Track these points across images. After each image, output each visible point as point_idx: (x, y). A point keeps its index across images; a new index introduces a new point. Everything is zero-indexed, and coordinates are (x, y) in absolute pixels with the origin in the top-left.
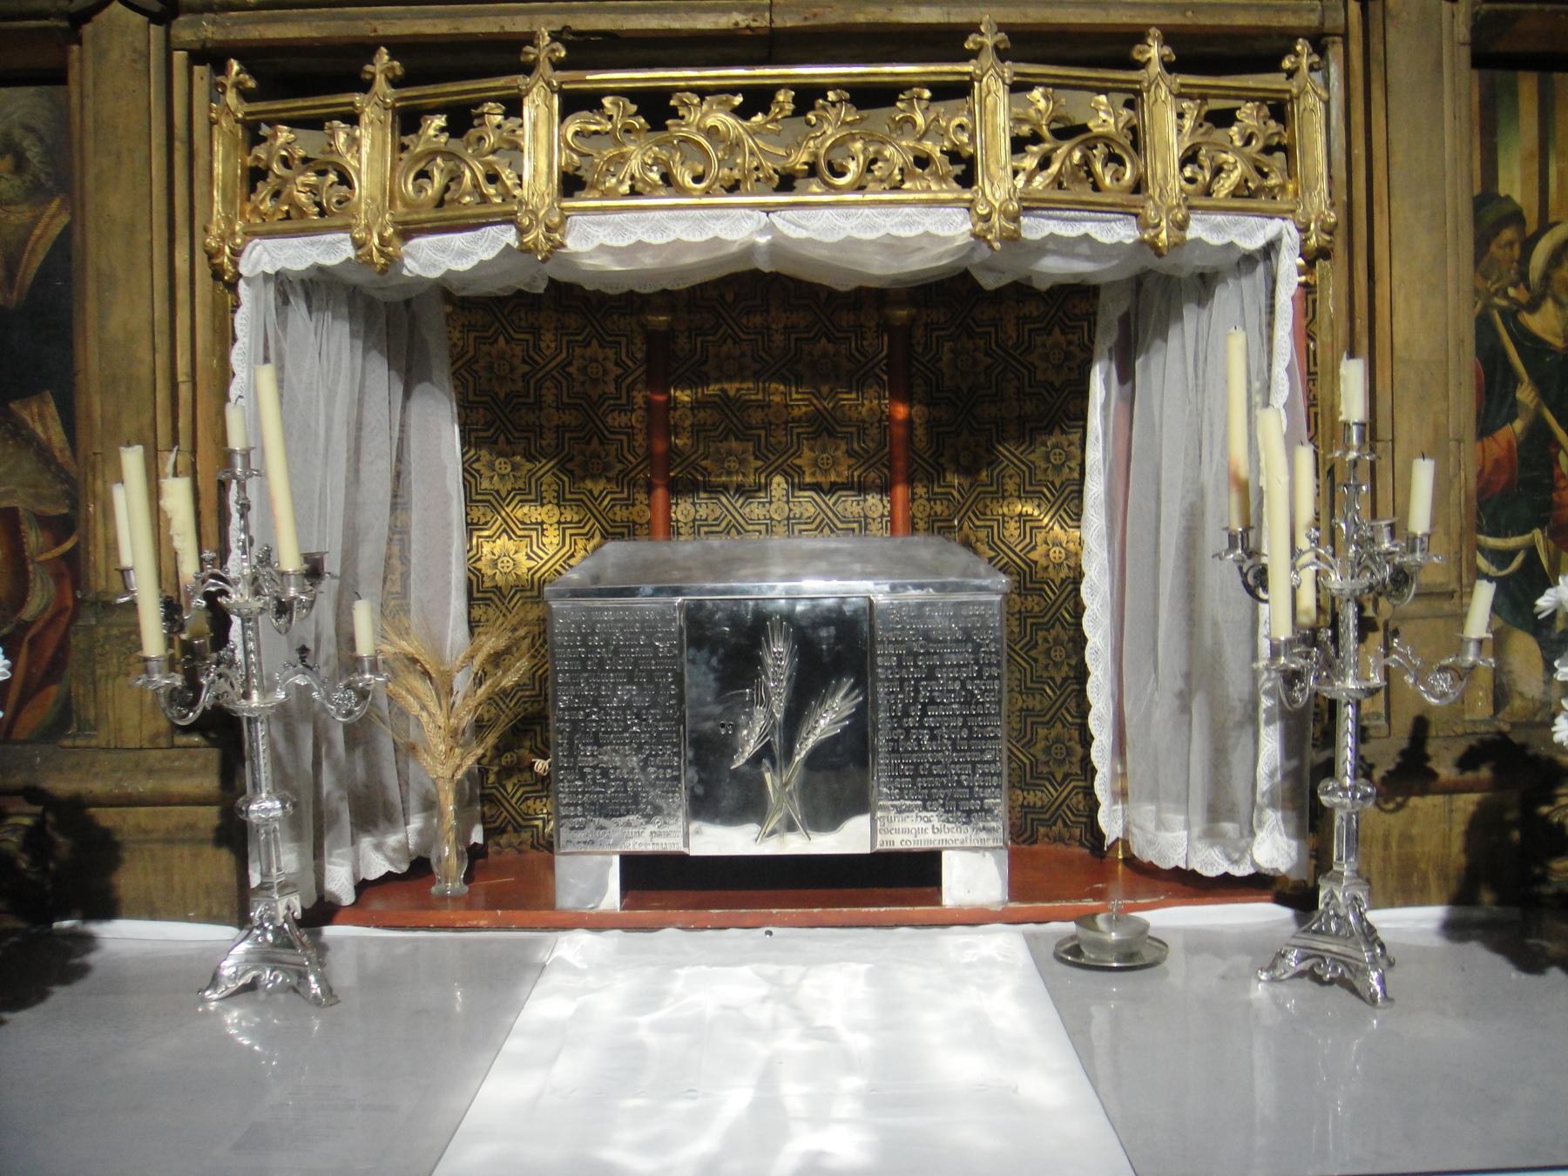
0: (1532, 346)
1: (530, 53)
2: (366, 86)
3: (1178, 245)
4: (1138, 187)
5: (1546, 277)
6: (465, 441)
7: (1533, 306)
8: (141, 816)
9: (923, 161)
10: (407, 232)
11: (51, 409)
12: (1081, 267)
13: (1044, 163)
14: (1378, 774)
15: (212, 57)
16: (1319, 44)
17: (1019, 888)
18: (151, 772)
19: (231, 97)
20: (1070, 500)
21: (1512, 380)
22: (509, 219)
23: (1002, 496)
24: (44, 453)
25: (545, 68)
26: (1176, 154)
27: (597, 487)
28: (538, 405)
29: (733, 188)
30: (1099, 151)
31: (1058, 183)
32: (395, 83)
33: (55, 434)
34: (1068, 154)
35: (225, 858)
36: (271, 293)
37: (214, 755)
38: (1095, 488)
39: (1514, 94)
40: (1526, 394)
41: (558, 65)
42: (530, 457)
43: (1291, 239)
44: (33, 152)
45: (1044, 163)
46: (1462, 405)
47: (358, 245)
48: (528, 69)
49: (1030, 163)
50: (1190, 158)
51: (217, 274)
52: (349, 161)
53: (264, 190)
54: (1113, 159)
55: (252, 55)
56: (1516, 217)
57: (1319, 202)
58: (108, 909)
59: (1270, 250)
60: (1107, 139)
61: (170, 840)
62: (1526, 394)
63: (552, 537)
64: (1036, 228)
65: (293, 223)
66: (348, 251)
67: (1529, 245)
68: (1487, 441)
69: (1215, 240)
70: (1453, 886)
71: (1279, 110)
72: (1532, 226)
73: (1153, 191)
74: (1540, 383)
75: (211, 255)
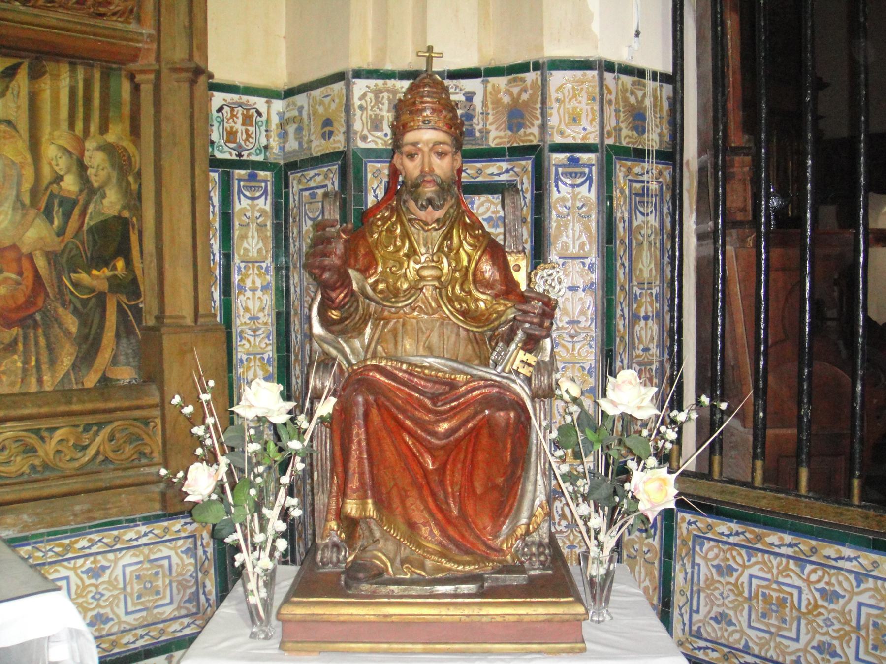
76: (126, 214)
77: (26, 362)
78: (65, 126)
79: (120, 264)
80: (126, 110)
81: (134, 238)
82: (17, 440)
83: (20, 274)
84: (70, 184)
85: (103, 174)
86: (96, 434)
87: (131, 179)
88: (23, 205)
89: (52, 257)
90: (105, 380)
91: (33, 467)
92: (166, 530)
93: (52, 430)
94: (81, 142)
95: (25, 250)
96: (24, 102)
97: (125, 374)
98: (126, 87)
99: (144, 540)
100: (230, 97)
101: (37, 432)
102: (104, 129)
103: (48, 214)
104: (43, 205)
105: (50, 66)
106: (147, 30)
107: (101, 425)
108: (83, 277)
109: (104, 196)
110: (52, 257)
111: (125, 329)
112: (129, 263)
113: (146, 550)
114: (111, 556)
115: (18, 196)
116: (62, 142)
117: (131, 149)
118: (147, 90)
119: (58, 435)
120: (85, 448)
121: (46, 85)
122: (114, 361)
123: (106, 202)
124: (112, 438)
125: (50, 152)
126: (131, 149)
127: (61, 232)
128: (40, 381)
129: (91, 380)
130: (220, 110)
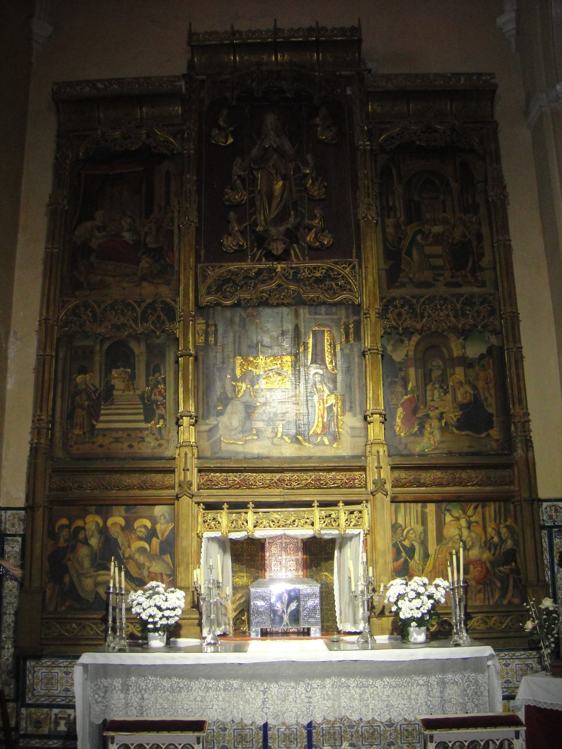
0: (404, 546)
1: (249, 506)
2: (223, 509)
3: (345, 534)
4: (338, 525)
5: (406, 536)
6: (233, 561)
7: (404, 540)
8: (186, 621)
9: (306, 522)
10: (229, 532)
11: (169, 557)
12: (331, 537)
13: (324, 522)
14: (376, 614)
15: (198, 503)
16: (367, 502)
17: (322, 635)
18: (188, 614)
19: (201, 510)
20: (332, 572)
21: (401, 552)
22: (246, 531)
23: (322, 571)
24: (168, 564)
25: (251, 508)
26: (344, 521)
27: (253, 570)
28: (243, 556)
29: (279, 527)
30: (333, 520)
31: (326, 526)
32: (228, 509)
33: (169, 561)
34: (328, 520)
35: (199, 628)
36: (207, 540)
37: (197, 612)
38: (336, 570)
39: (400, 507)
40: (403, 554)
41: (253, 508)
42: (242, 565)
43: (362, 532)
44: (167, 515)
45: (324, 522)
46: (390, 557)
47: (222, 533)
48: (248, 508)
49: (322, 522)
50: (347, 520)
51: (198, 537)
52: (220, 520)
53: (206, 524)
54: (335, 521)
55: (204, 503)
56: (401, 526)
57: (366, 526)
58: (179, 636)
59: (359, 533)
60: (334, 518)
61: (190, 625)
62: (403, 554)
63: (245, 579)
64: (323, 532)
65: (211, 529)
66: (221, 534)
67: (403, 530)
68: (395, 563)
69: (351, 533)
70: (390, 632)
71: (360, 512)
72: (404, 527)
73: (341, 526)
74: (406, 553)
75: (197, 534)
76: (515, 548)
77: (485, 596)
78: (493, 522)
79: (513, 564)
80: (512, 513)
81: (517, 555)
82: (482, 619)
83: (482, 568)
84: (496, 539)
85: (506, 535)
86: (506, 619)
87: (515, 536)
88: (482, 547)
89: (490, 562)
90: (510, 602)
91: (487, 628)
92: (531, 654)
93: (492, 617)
94: (498, 526)
95: (483, 560)
96: (481, 516)
97: (516, 601)
98: (512, 506)
99: (523, 657)
100: (549, 503)
101: (488, 617)
102: (505, 521)
103: (490, 549)
104: (488, 547)
105: (488, 503)
106: (517, 488)
107: (508, 616)
108: (502, 569)
109: (507, 542)
110: (491, 562)
111: (515, 586)
112: (516, 562)
113: (524, 660)
114: (511, 660)
115: (480, 545)
116: (493, 526)
117: (515, 526)
118: (518, 508)
119: (495, 618)
120: (502, 623)
121: (487, 509)
122: (513, 596)
123: (508, 544)
124: (511, 621)
125: (489, 530)
126: (515, 526)
127: (494, 554)
128: (489, 602)
129: (505, 602)
130: (546, 508)
